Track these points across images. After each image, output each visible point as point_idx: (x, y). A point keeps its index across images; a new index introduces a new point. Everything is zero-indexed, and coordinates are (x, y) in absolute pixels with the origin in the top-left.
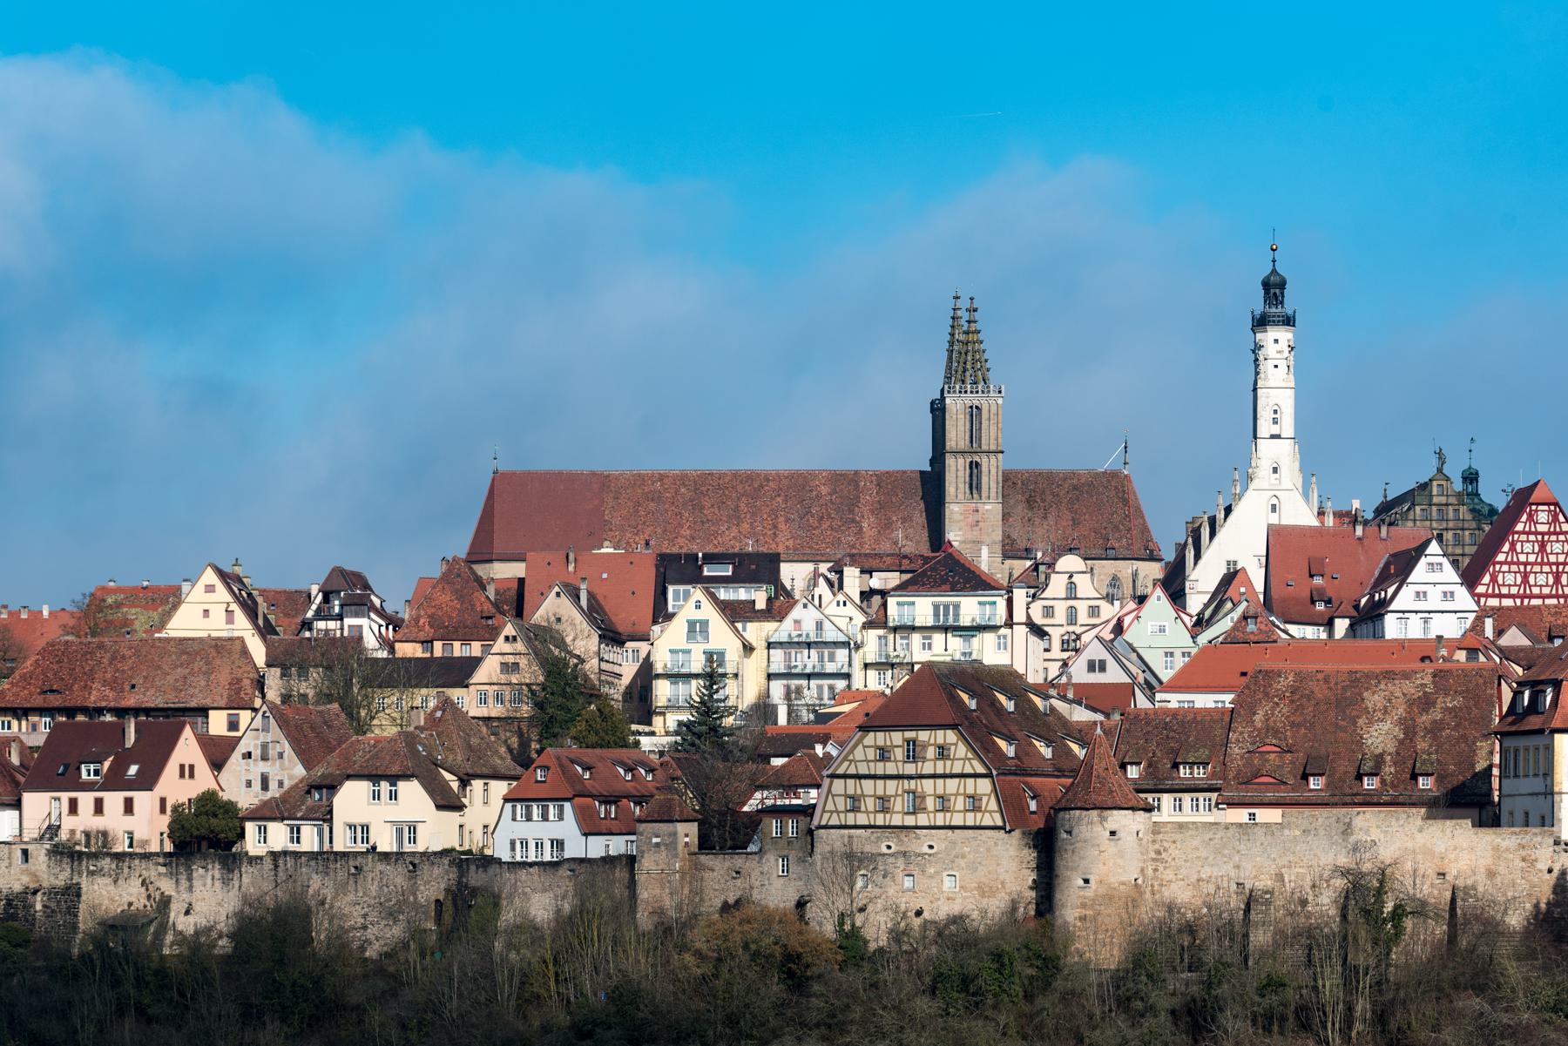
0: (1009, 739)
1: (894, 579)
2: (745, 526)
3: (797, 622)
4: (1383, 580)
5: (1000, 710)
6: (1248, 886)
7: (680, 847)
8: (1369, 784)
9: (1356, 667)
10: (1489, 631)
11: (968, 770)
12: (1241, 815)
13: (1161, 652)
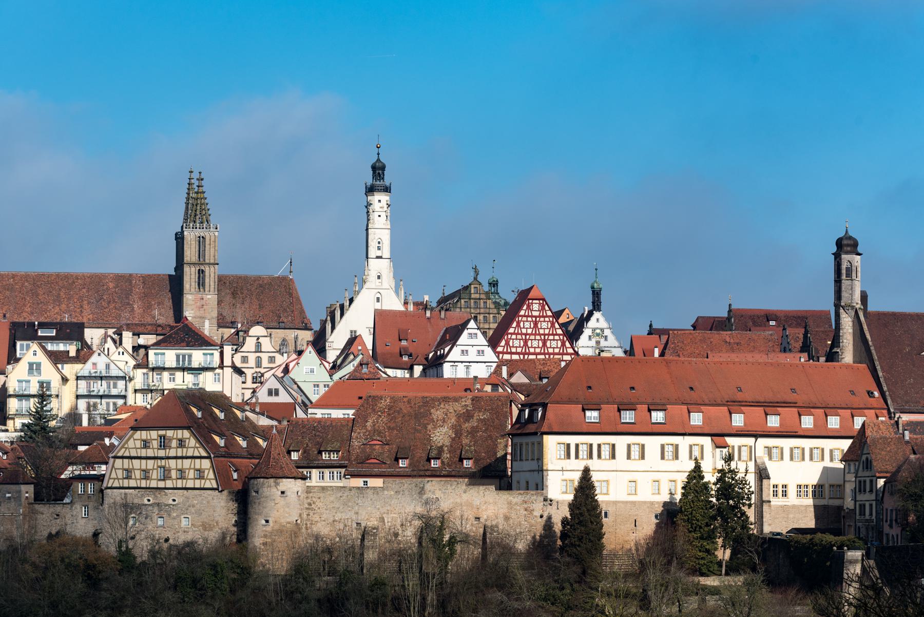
0: (221, 435)
1: (150, 339)
2: (64, 306)
3: (94, 364)
4: (442, 343)
5: (215, 418)
6: (363, 525)
7: (23, 500)
8: (434, 464)
9: (426, 394)
10: (505, 374)
11: (197, 454)
12: (359, 482)
13: (312, 385)
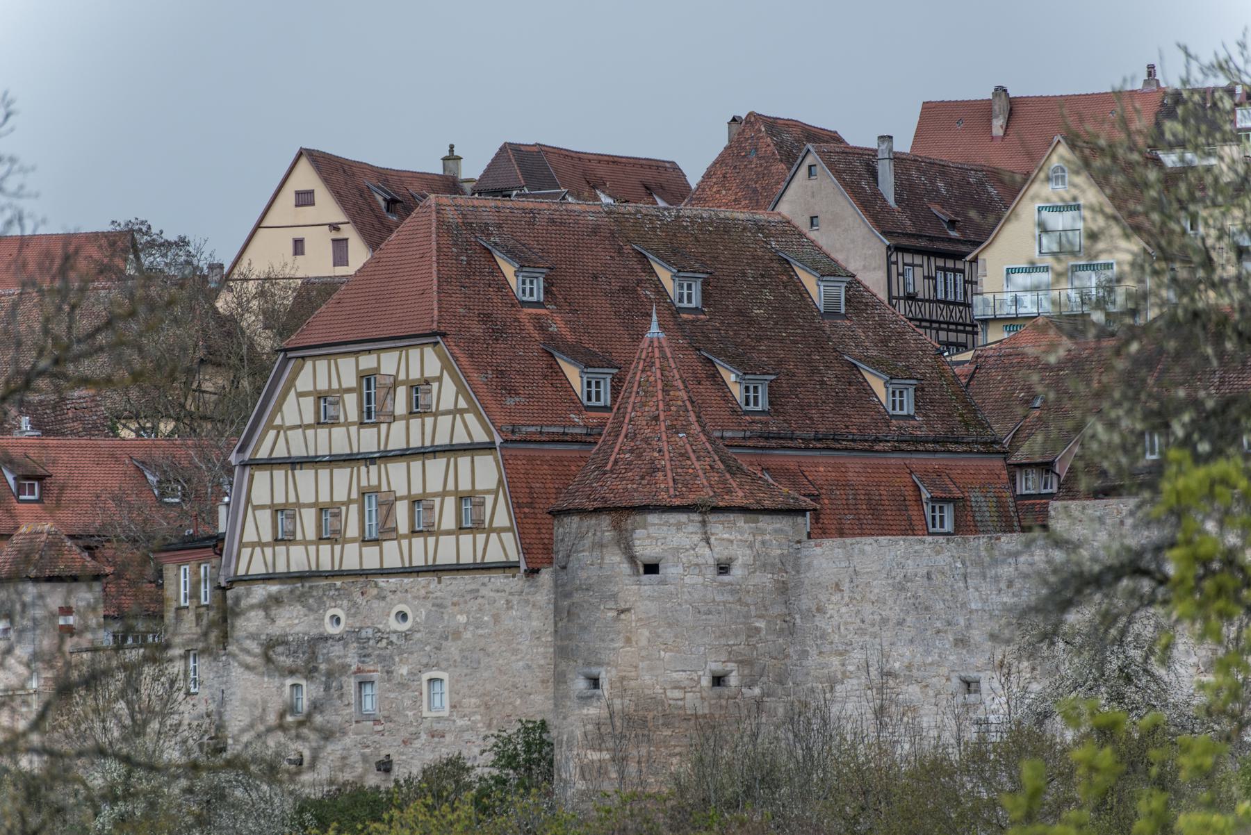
11: (461, 438)
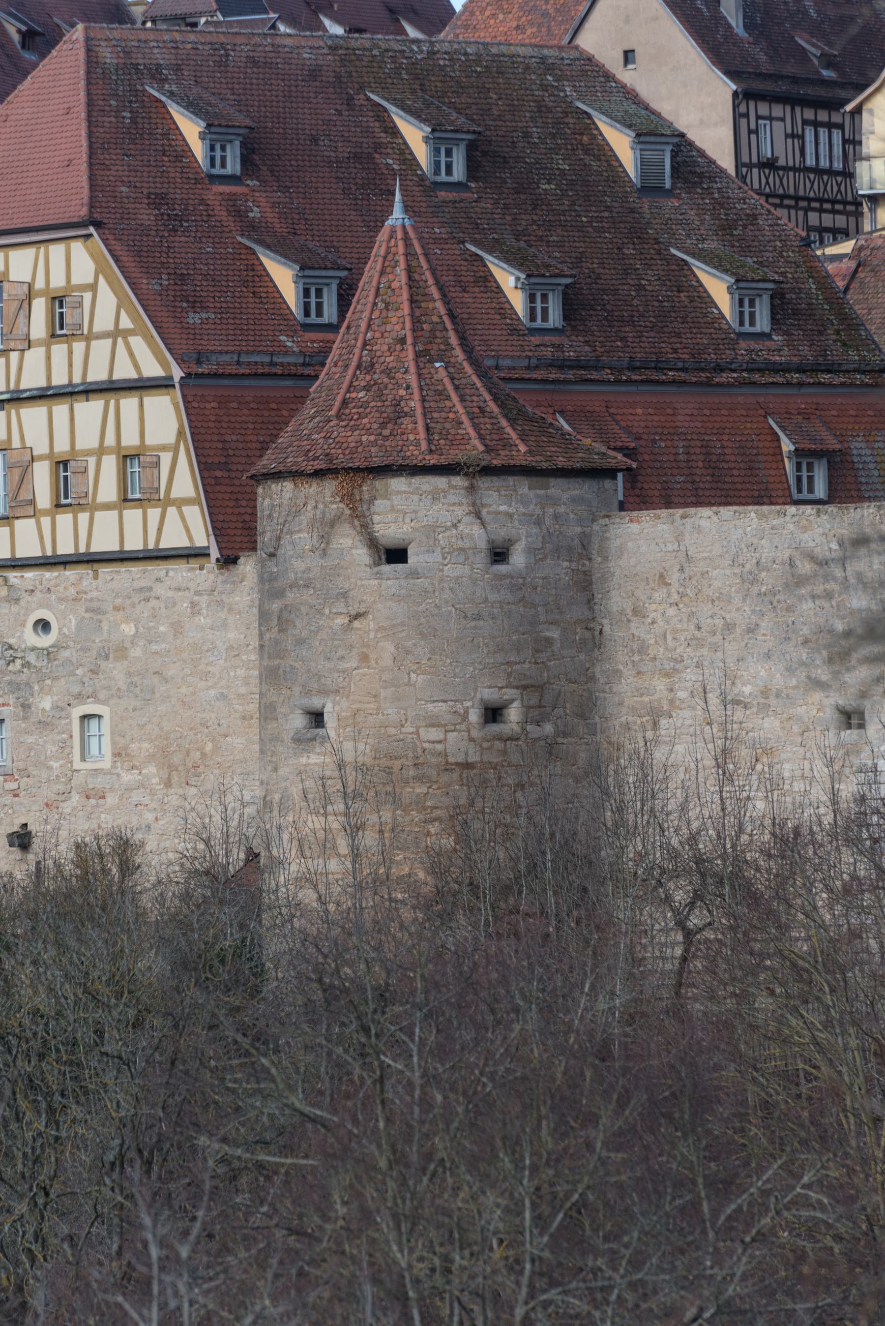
11: (124, 372)
